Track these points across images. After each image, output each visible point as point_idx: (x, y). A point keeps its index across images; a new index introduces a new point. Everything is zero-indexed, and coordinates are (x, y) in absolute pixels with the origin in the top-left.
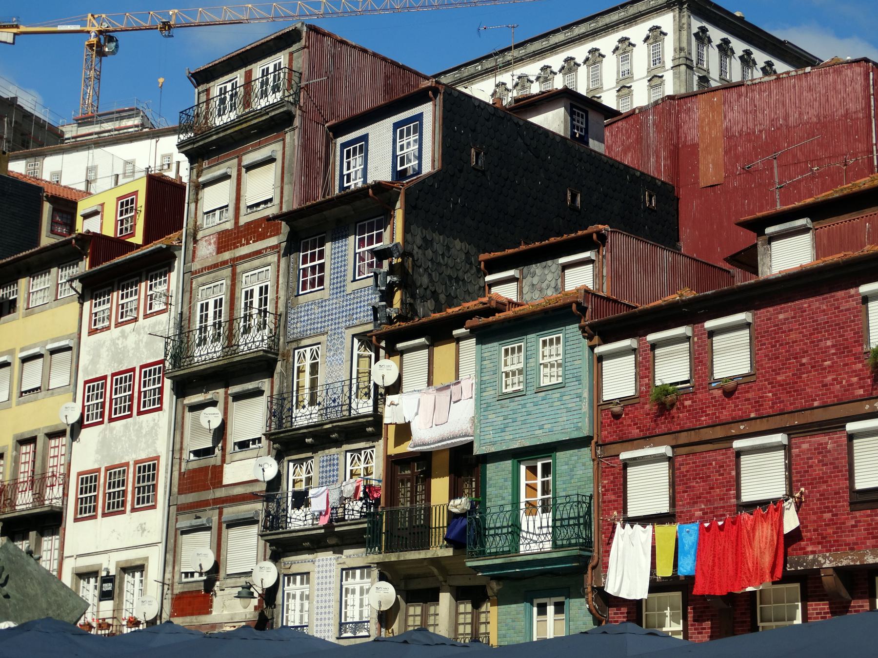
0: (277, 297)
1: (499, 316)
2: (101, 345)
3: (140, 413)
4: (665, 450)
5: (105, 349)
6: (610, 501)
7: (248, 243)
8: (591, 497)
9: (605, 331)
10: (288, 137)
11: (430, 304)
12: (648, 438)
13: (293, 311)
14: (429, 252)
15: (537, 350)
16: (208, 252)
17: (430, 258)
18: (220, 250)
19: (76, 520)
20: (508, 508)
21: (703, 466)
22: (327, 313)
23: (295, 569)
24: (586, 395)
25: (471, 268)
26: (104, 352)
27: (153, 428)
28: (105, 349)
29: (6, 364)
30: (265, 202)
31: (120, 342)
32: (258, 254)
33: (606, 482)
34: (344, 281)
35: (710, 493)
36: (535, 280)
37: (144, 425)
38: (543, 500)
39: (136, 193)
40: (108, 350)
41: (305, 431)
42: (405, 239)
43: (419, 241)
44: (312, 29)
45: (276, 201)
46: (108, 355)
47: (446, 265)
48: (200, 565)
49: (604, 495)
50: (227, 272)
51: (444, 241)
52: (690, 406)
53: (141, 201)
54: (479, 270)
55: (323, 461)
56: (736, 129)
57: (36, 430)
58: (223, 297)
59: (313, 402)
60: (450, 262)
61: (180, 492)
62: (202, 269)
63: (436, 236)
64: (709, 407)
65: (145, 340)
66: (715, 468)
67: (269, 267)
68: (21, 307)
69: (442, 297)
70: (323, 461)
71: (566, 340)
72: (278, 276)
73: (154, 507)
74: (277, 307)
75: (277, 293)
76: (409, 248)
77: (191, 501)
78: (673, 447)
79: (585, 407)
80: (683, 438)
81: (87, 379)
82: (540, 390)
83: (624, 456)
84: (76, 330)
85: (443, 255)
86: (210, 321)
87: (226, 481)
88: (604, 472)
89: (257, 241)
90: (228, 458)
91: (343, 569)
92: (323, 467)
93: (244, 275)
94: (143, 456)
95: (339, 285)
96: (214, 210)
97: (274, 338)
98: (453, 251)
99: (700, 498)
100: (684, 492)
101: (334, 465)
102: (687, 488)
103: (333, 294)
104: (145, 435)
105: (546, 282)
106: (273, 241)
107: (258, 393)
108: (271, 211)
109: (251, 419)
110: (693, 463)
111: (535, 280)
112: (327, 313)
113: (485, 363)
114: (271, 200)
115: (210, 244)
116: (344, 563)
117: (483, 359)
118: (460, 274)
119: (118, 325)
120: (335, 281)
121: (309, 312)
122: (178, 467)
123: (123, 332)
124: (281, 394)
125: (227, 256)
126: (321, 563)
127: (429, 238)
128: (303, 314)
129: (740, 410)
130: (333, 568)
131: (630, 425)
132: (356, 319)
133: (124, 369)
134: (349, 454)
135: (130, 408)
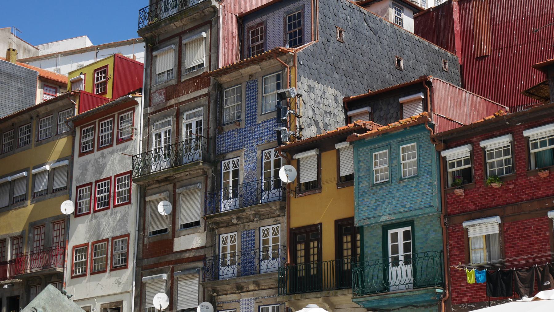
0: (208, 127)
1: (369, 132)
2: (88, 163)
3: (115, 206)
4: (497, 220)
5: (90, 165)
6: (456, 255)
7: (187, 93)
8: (441, 251)
11: (314, 129)
12: (482, 212)
13: (220, 136)
14: (312, 94)
15: (399, 154)
16: (160, 100)
17: (313, 99)
18: (168, 99)
19: (72, 278)
20: (381, 261)
21: (524, 229)
22: (244, 137)
24: (435, 183)
25: (338, 106)
26: (90, 167)
27: (124, 216)
28: (90, 165)
29: (24, 178)
30: (199, 66)
31: (100, 160)
33: (451, 242)
34: (255, 115)
35: (531, 247)
36: (382, 114)
38: (405, 256)
39: (107, 66)
40: (92, 166)
43: (306, 88)
46: (92, 170)
48: (160, 305)
49: (450, 251)
51: (321, 88)
52: (513, 188)
53: (110, 71)
55: (244, 234)
56: (498, 20)
57: (44, 219)
58: (171, 128)
59: (235, 195)
64: (527, 188)
65: (117, 159)
66: (534, 230)
67: (202, 108)
68: (33, 141)
69: (321, 125)
70: (244, 234)
71: (419, 147)
72: (209, 113)
73: (125, 267)
74: (208, 134)
75: (208, 125)
79: (436, 193)
81: (78, 185)
82: (401, 180)
84: (70, 154)
85: (321, 97)
86: (163, 145)
87: (176, 248)
88: (451, 235)
90: (176, 234)
91: (259, 307)
92: (244, 238)
93: (186, 114)
94: (118, 234)
95: (251, 118)
96: (163, 73)
99: (523, 251)
100: (511, 247)
101: (251, 237)
102: (513, 244)
103: (248, 124)
105: (390, 114)
106: (205, 91)
109: (192, 209)
110: (517, 227)
111: (382, 114)
112: (244, 137)
113: (361, 164)
114: (203, 64)
115: (161, 95)
117: (359, 162)
119: (99, 149)
120: (249, 115)
121: (231, 136)
122: (142, 241)
123: (103, 154)
124: (212, 190)
125: (173, 102)
126: (244, 302)
128: (227, 138)
129: (550, 189)
130: (252, 305)
131: (468, 203)
132: (265, 139)
133: (104, 178)
134: (262, 229)
135: (108, 203)
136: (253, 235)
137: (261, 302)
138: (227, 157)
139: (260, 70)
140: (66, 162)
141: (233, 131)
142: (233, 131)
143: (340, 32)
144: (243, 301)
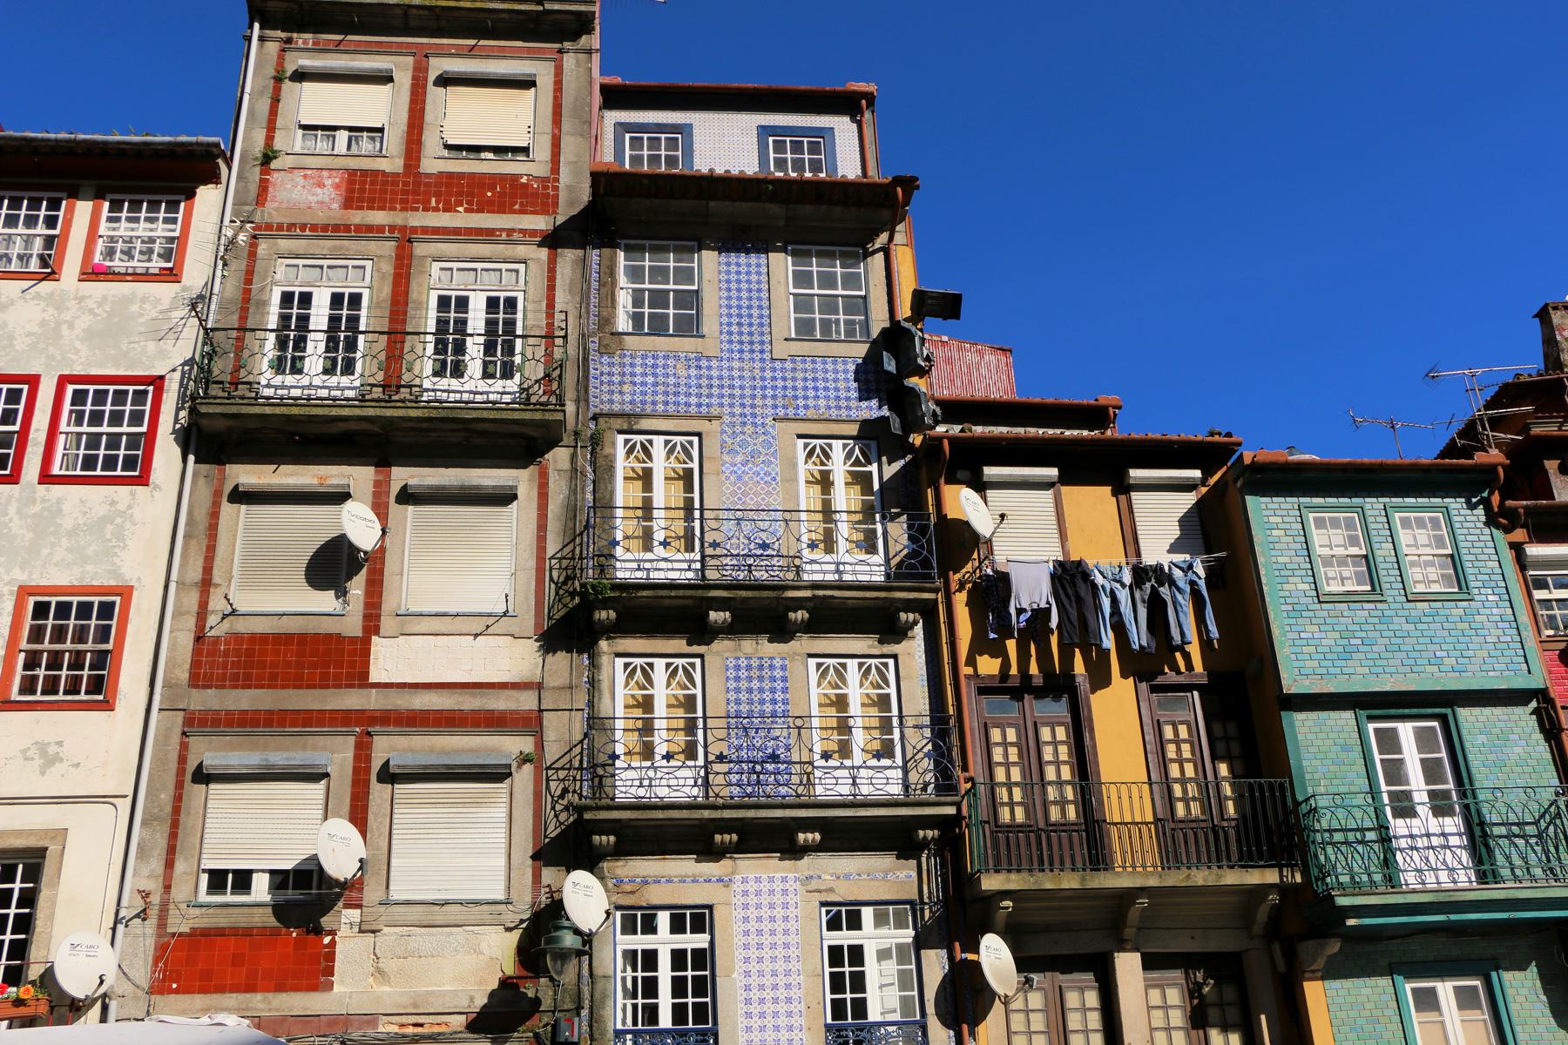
10: (569, 61)
13: (605, 359)
18: (348, 204)
23: (655, 895)
27: (104, 520)
30: (499, 150)
32: (487, 235)
37: (66, 507)
41: (724, 594)
45: (542, 153)
50: (389, 248)
61: (198, 679)
62: (291, 226)
72: (551, 288)
77: (244, 705)
87: (375, 676)
89: (478, 211)
90: (386, 623)
104: (73, 533)
107: (504, 498)
108: (532, 169)
114: (525, 150)
115: (321, 185)
116: (831, 890)
125: (378, 217)
128: (638, 370)
136: (778, 673)
137: (831, 890)
138: (645, 424)
139: (781, 223)
141: (666, 357)
142: (666, 357)
144: (745, 880)
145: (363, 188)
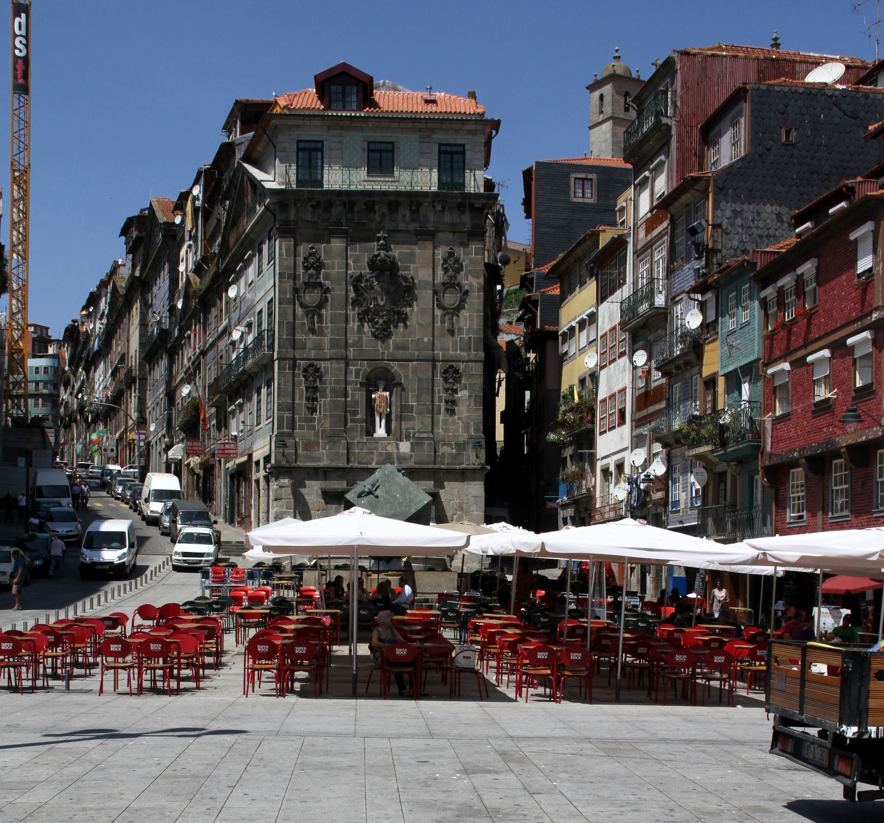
9: (765, 279)
12: (782, 358)
14: (739, 221)
18: (648, 232)
19: (601, 433)
32: (660, 236)
42: (713, 216)
43: (728, 213)
44: (685, 53)
47: (757, 227)
54: (790, 225)
60: (761, 224)
63: (745, 206)
76: (718, 221)
78: (791, 364)
80: (794, 357)
83: (770, 371)
85: (753, 220)
97: (667, 297)
98: (764, 215)
106: (665, 224)
118: (771, 232)
127: (738, 209)
138: (677, 299)
140: (593, 309)
143: (788, 133)
145: (651, 224)
